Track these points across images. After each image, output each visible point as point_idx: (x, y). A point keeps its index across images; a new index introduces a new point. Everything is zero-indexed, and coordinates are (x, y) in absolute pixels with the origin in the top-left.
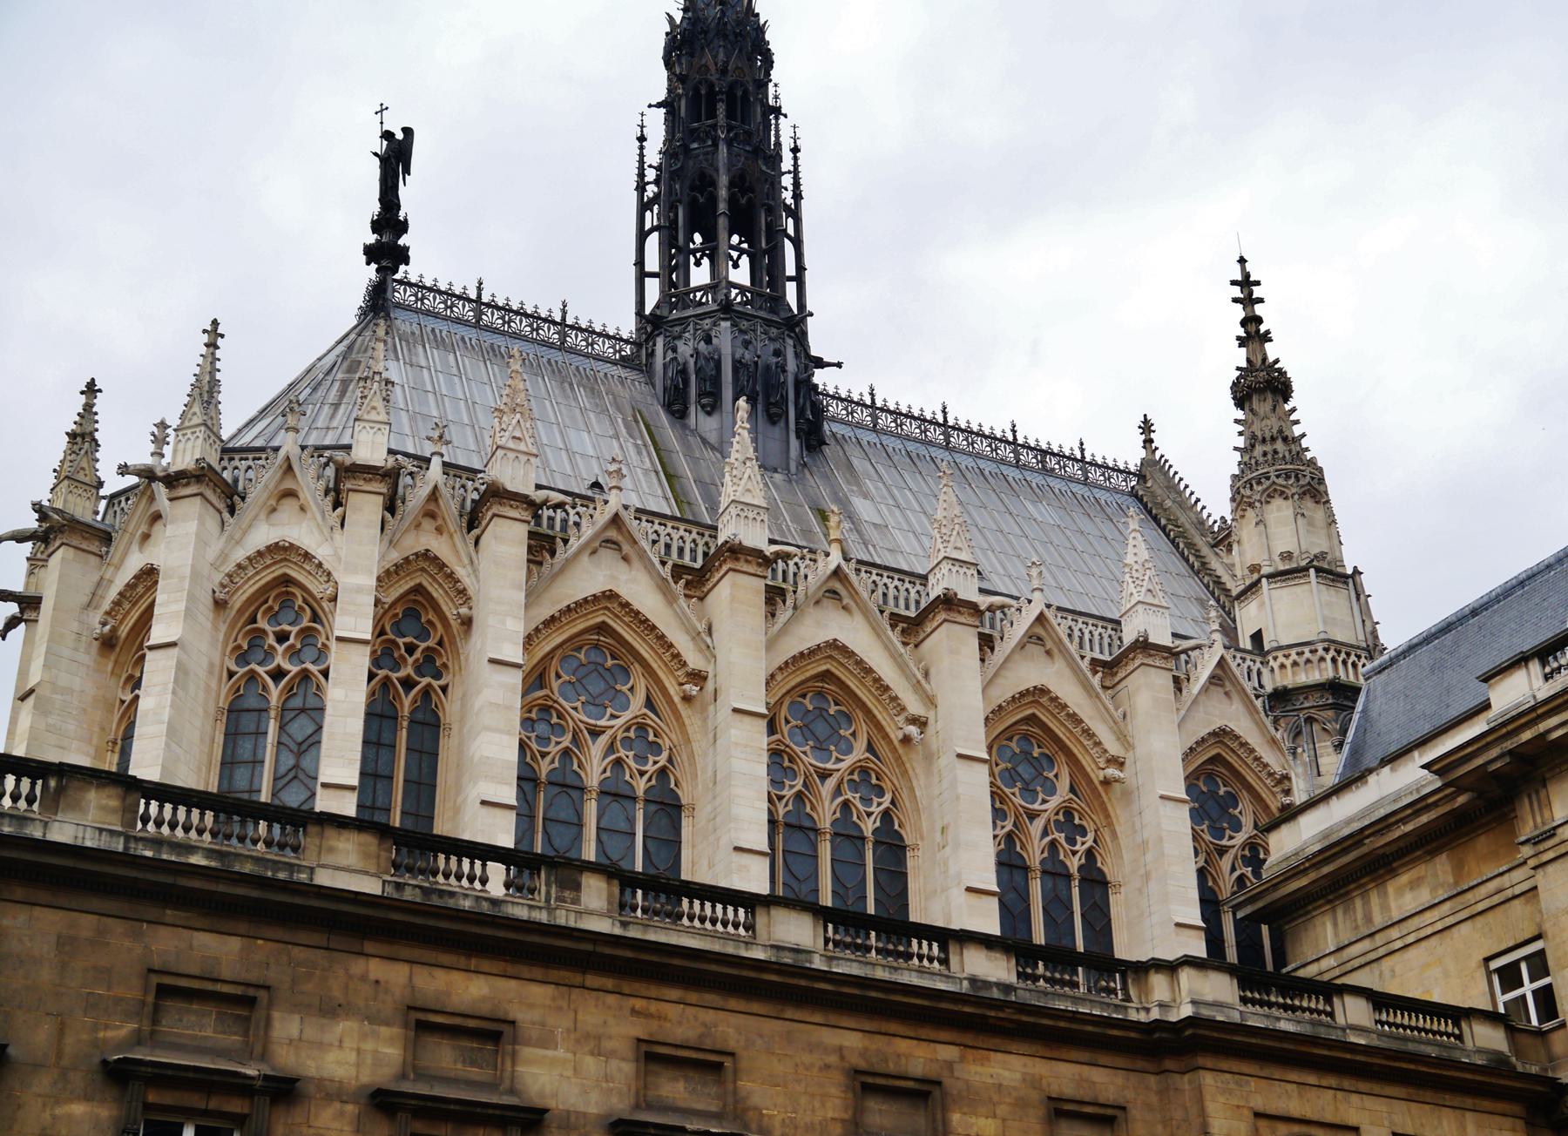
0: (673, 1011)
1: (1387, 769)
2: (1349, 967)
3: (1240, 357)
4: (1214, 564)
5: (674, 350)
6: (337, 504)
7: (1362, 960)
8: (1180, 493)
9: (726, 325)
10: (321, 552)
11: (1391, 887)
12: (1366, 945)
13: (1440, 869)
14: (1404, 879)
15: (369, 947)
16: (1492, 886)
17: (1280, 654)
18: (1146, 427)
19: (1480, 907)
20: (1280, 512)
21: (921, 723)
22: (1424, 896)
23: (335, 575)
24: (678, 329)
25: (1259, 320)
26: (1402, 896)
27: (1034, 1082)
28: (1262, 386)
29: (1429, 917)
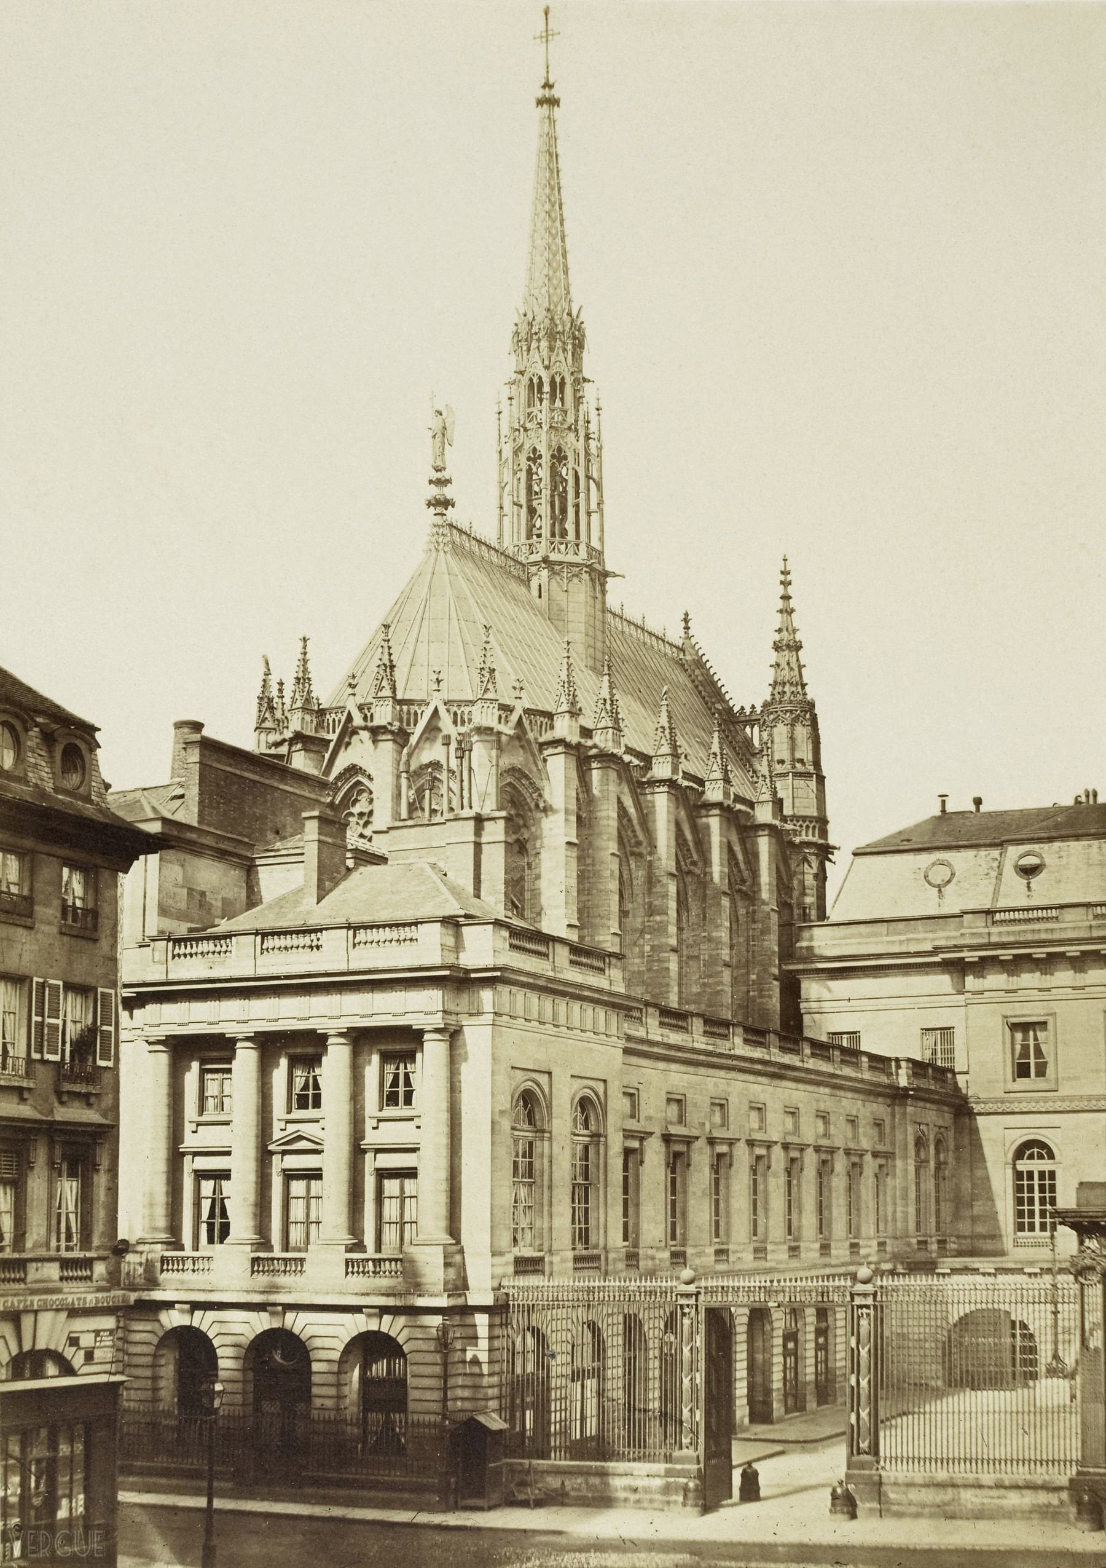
3: (777, 620)
18: (686, 620)
21: (694, 863)
25: (790, 598)
27: (872, 1113)
28: (789, 646)
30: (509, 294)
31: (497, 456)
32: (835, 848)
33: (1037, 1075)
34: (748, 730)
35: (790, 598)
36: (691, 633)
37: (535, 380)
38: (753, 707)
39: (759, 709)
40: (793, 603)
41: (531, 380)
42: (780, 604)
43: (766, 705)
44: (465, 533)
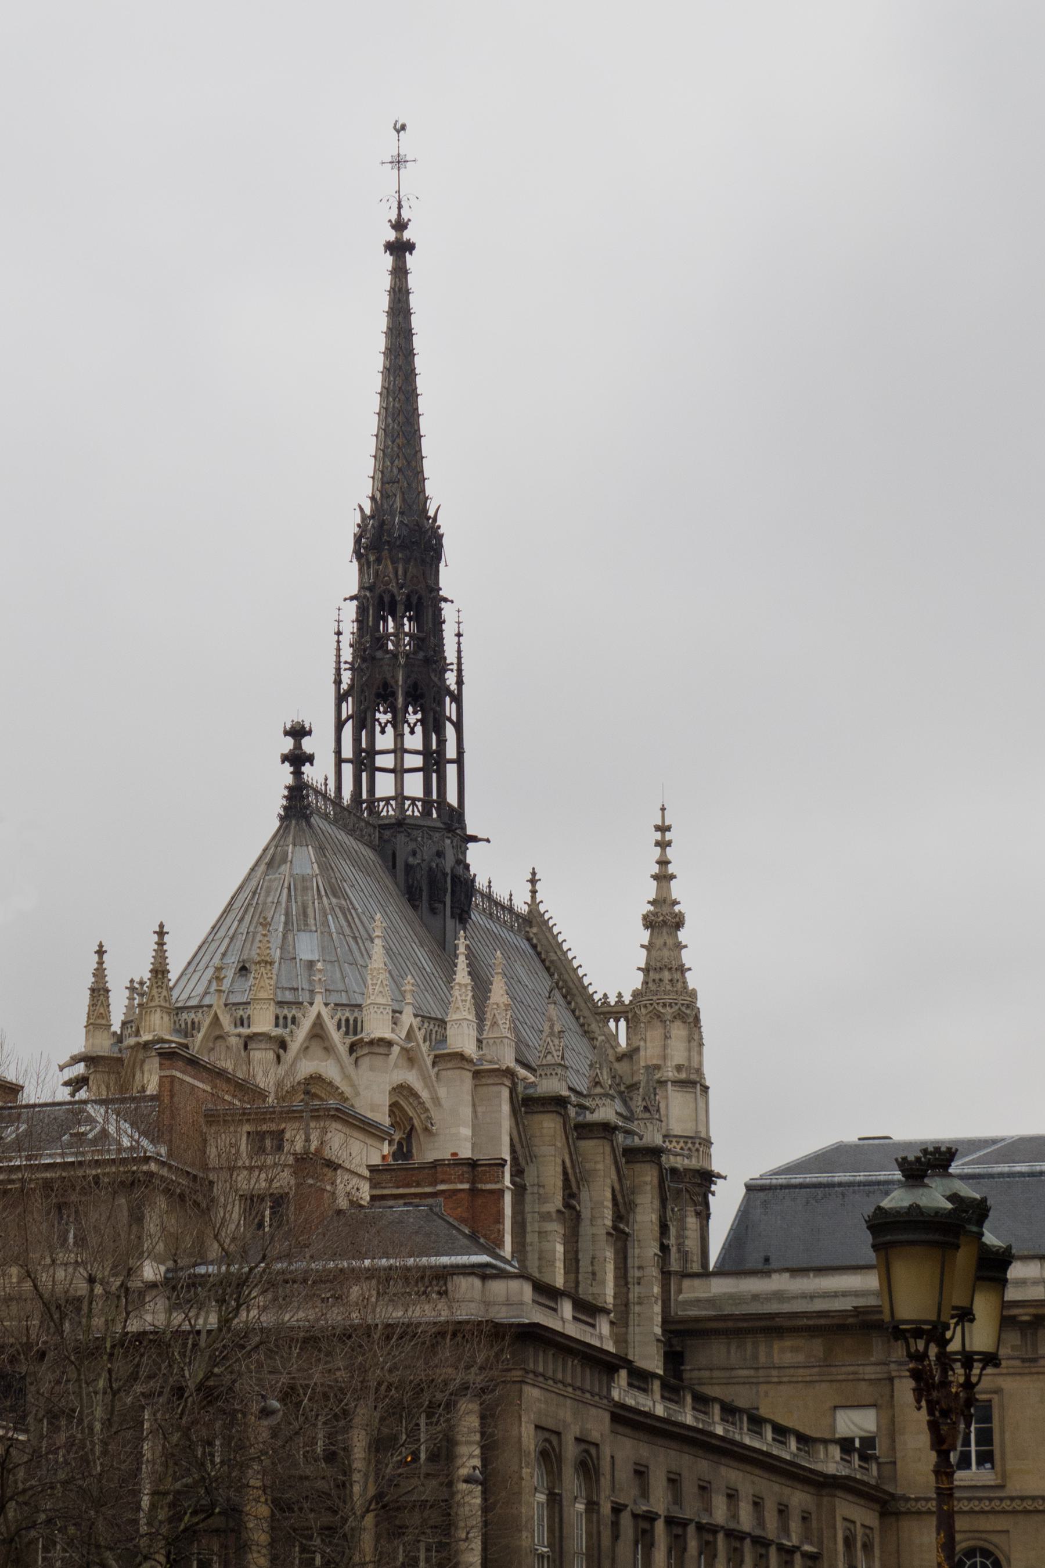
0: (756, 1479)
1: (787, 1275)
2: (735, 1380)
3: (651, 889)
4: (594, 1027)
5: (414, 854)
6: (434, 1064)
7: (746, 1380)
8: (565, 953)
9: (448, 841)
10: (425, 1095)
11: (777, 1345)
12: (752, 1372)
13: (817, 1346)
14: (788, 1343)
15: (723, 1461)
16: (851, 1369)
17: (674, 1140)
18: (533, 881)
19: (840, 1377)
20: (678, 1031)
22: (800, 1358)
23: (434, 1113)
24: (415, 832)
25: (669, 862)
26: (785, 1353)
28: (664, 921)
29: (801, 1371)
30: (352, 486)
31: (332, 687)
32: (719, 1176)
33: (980, 1464)
34: (612, 1024)
35: (669, 862)
36: (539, 897)
37: (387, 599)
38: (620, 995)
39: (627, 999)
40: (671, 869)
41: (381, 598)
42: (656, 869)
43: (636, 994)
44: (321, 794)
